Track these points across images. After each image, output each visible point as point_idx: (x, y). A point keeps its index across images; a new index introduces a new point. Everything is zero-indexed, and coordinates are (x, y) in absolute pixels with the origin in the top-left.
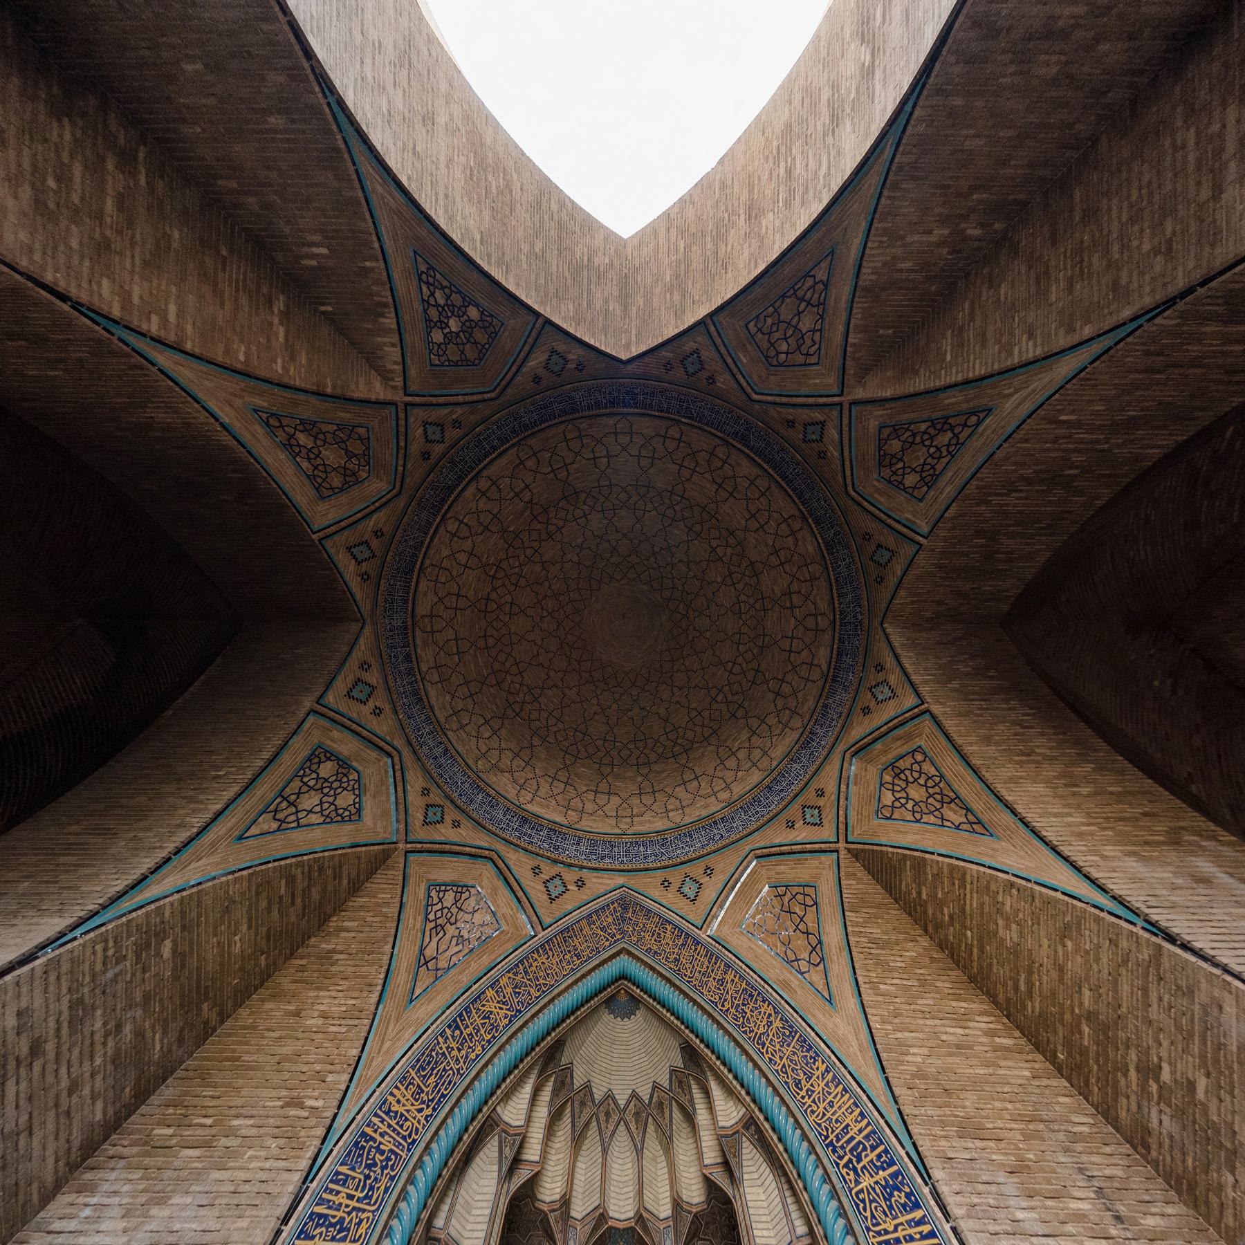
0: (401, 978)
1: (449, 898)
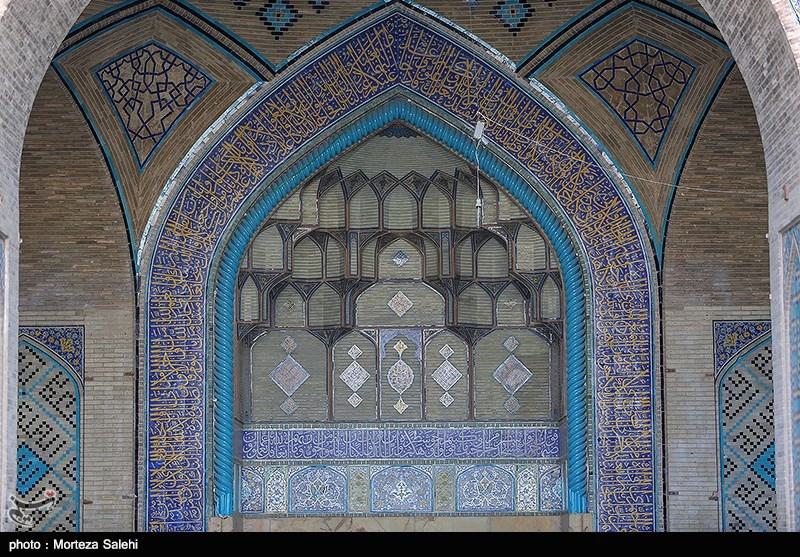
0: (121, 157)
1: (126, 71)
